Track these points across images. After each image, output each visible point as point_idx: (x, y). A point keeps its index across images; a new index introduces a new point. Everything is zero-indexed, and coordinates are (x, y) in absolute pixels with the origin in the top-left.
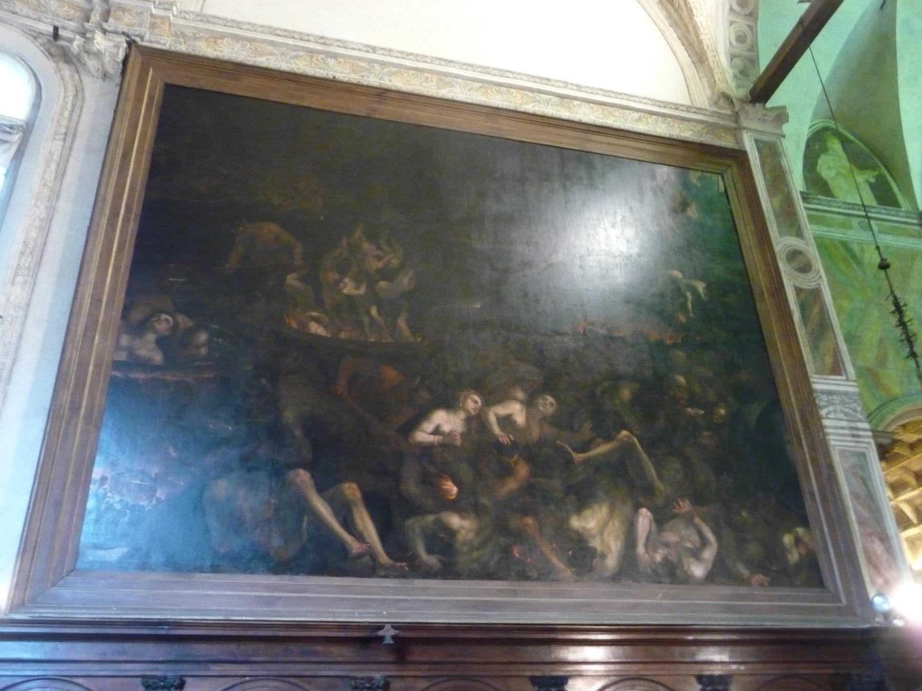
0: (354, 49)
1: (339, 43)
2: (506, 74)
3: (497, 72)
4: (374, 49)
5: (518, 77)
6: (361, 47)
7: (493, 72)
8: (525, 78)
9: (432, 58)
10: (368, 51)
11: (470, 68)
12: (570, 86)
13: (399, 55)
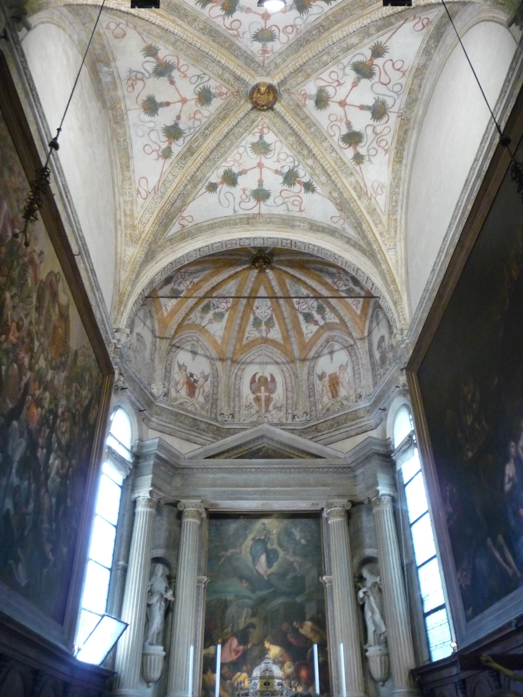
0: (432, 279)
1: (428, 284)
2: (459, 206)
3: (457, 211)
4: (433, 270)
5: (462, 198)
6: (432, 276)
7: (456, 213)
8: (463, 195)
9: (443, 243)
10: (434, 273)
11: (452, 226)
12: (474, 166)
13: (438, 260)
